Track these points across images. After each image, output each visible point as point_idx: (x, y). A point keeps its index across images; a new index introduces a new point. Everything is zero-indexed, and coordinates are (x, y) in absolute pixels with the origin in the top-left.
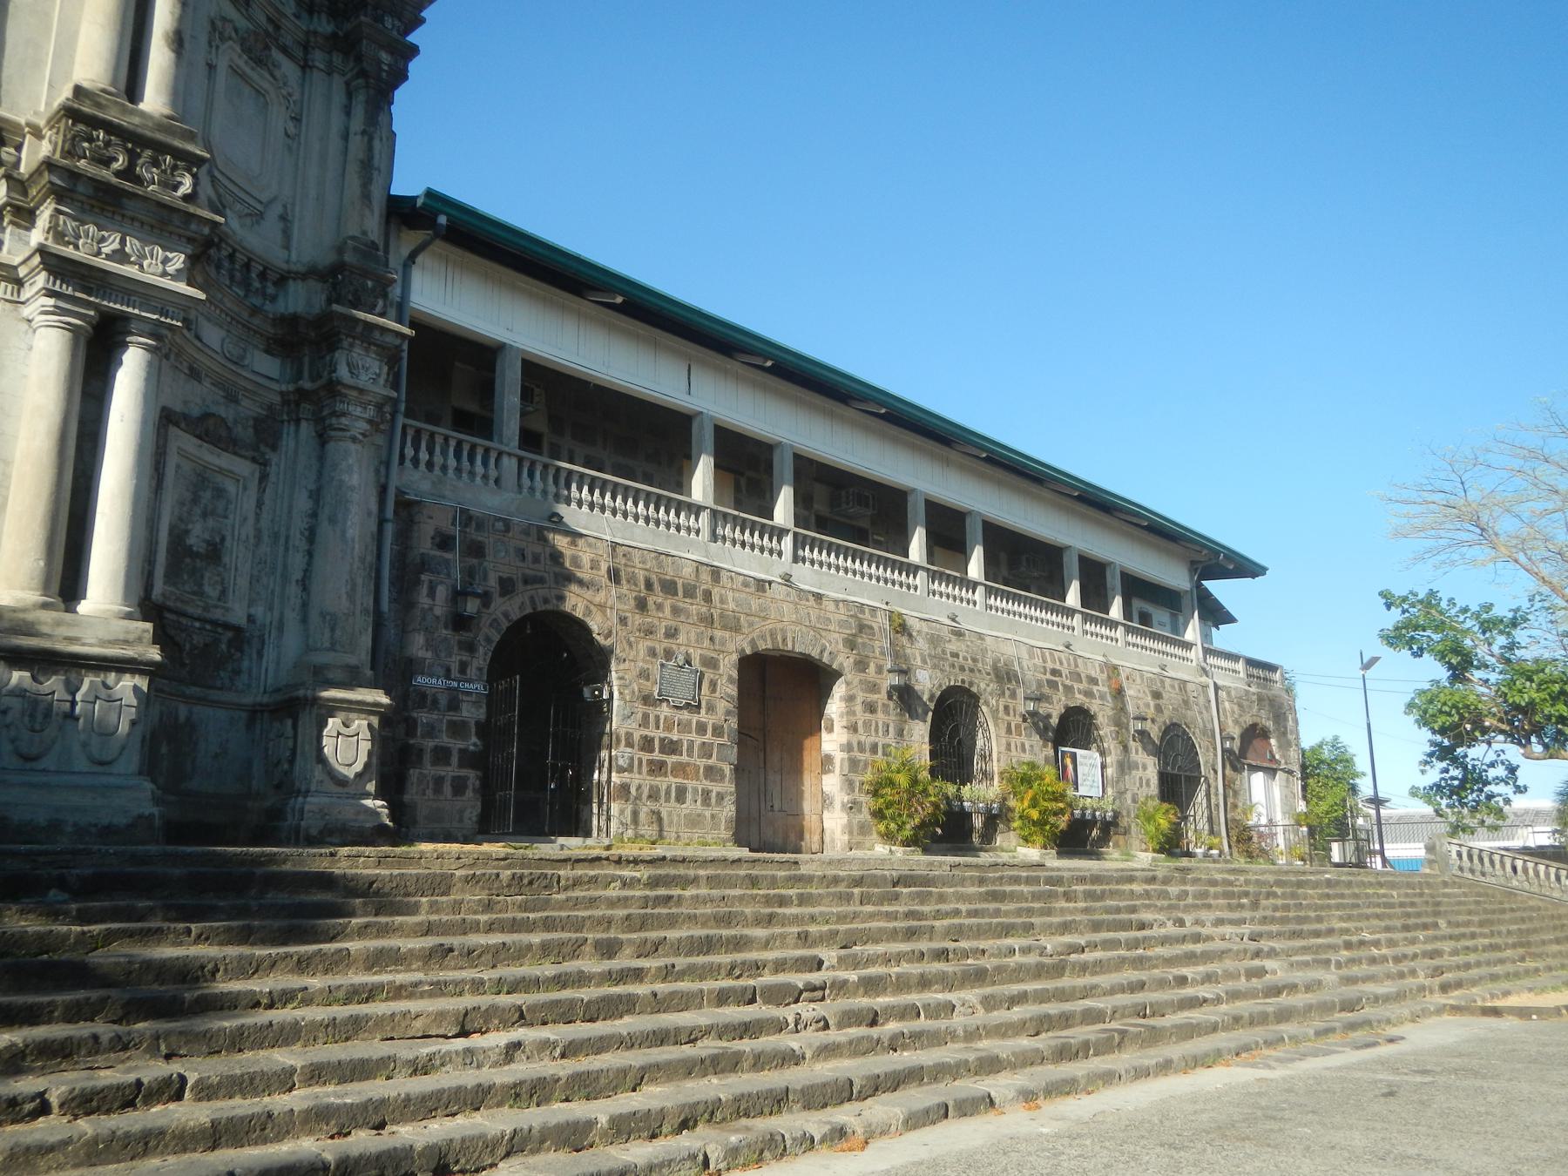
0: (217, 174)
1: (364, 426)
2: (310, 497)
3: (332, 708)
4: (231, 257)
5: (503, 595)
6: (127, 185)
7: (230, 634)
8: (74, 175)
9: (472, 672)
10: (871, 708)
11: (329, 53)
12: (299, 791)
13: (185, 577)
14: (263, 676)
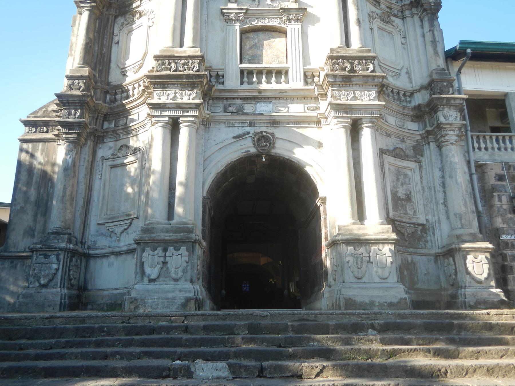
0: (381, 64)
1: (456, 138)
2: (440, 170)
3: (468, 252)
4: (392, 91)
6: (352, 74)
7: (421, 227)
8: (335, 76)
11: (411, 10)
12: (462, 287)
13: (400, 208)
14: (437, 242)
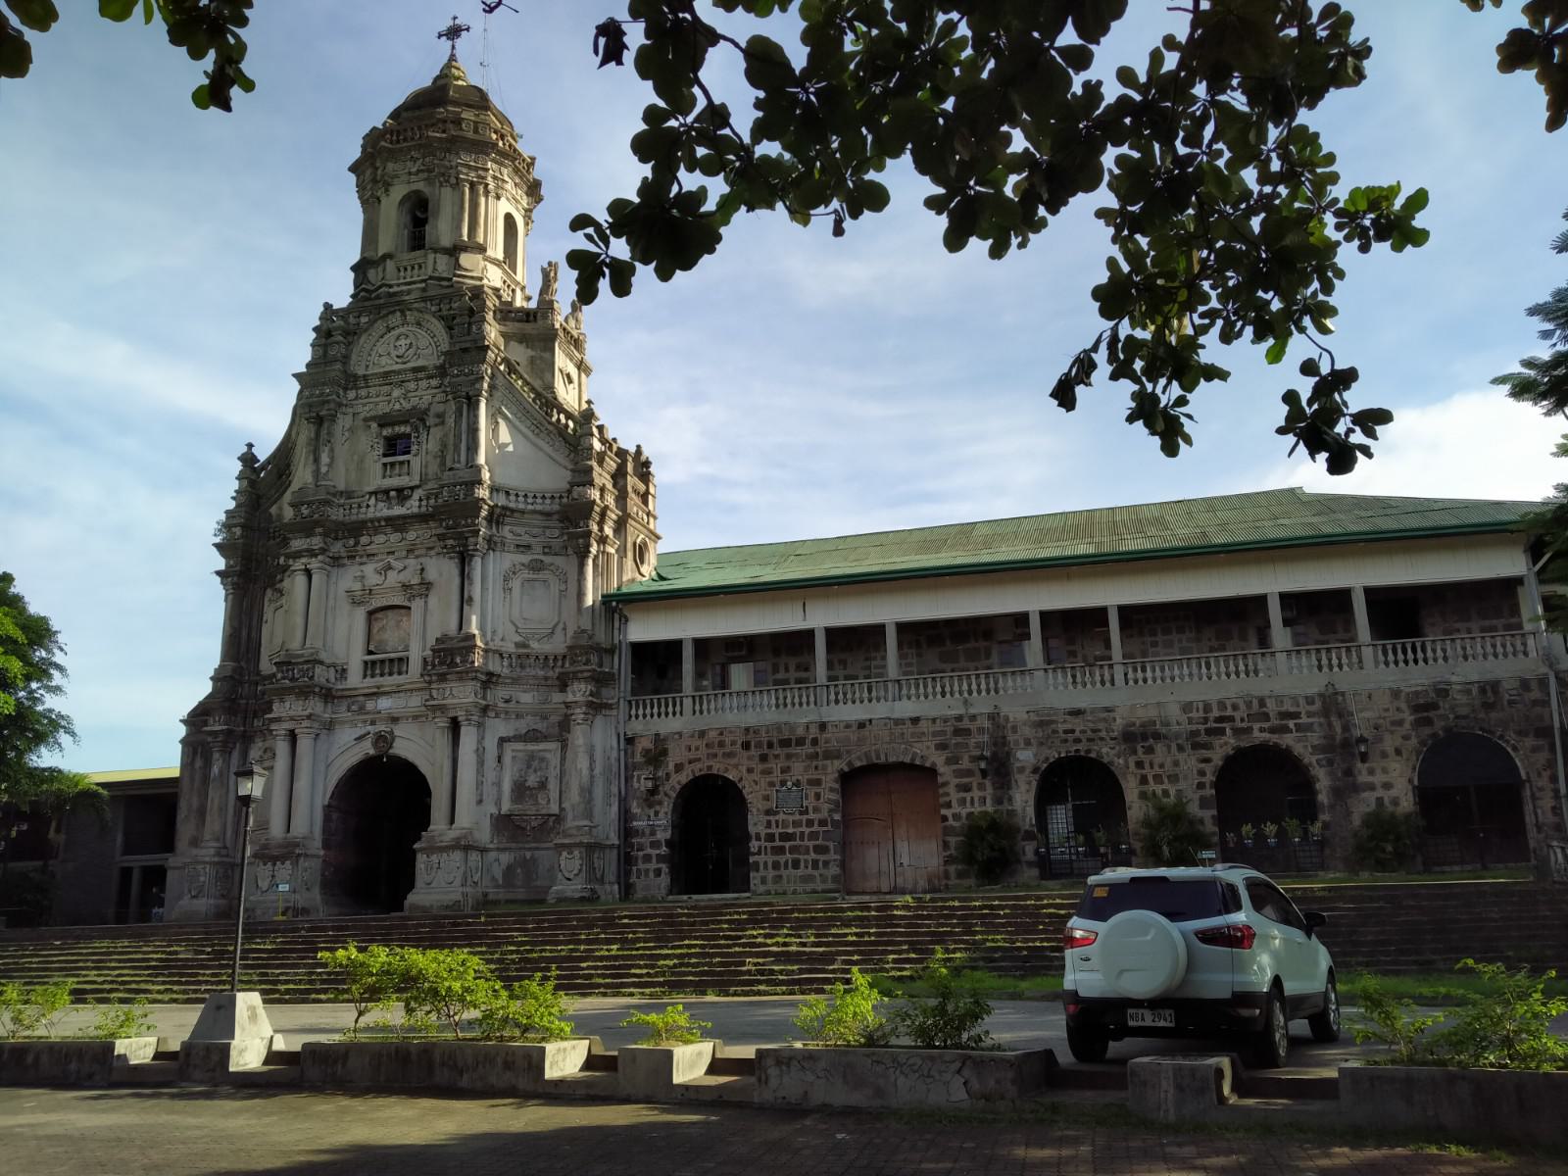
5: (676, 772)
9: (661, 815)
10: (967, 788)
